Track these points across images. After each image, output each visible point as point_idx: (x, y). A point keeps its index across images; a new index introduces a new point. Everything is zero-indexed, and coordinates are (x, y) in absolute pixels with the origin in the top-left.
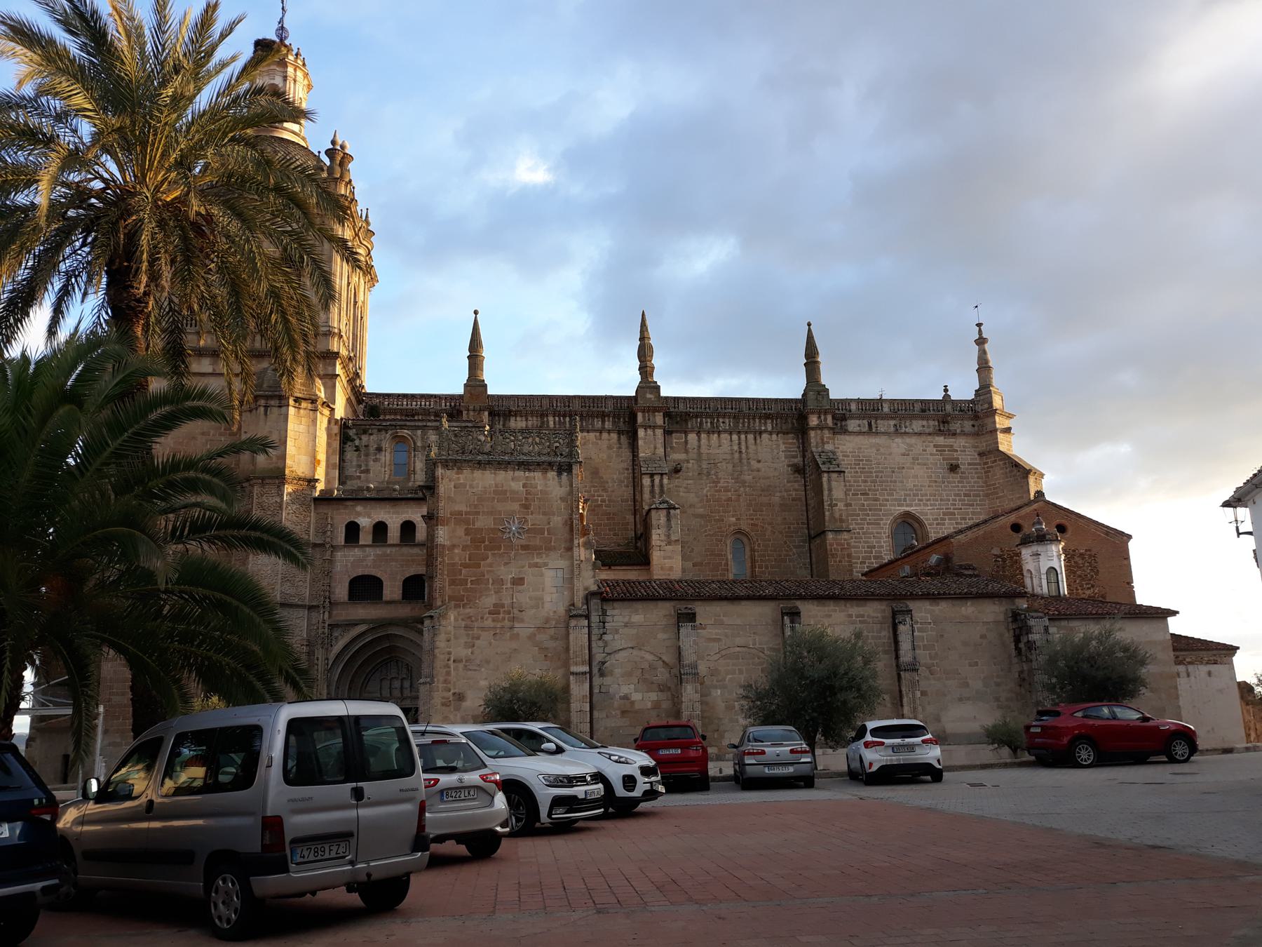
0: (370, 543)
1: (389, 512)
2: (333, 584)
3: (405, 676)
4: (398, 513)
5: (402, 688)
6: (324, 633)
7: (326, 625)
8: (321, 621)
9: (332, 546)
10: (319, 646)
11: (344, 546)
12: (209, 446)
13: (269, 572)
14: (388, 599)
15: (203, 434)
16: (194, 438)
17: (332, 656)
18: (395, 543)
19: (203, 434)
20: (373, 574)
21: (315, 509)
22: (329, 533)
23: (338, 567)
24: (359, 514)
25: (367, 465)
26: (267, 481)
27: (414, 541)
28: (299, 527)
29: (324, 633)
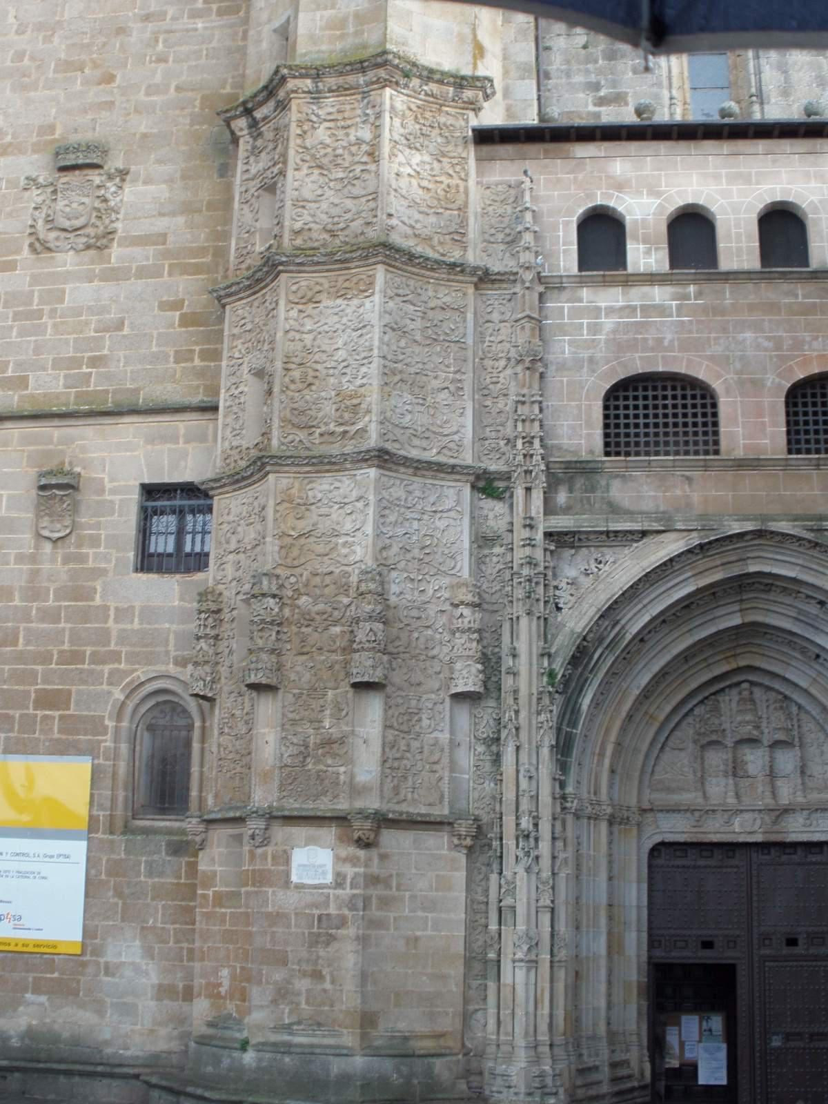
0: (665, 267)
1: (717, 177)
2: (550, 403)
3: (780, 736)
4: (747, 179)
5: (772, 775)
6: (531, 562)
7: (539, 536)
8: (518, 521)
9: (540, 279)
10: (518, 609)
11: (581, 282)
12: (160, 46)
13: (341, 354)
14: (740, 453)
15: (147, 18)
16: (121, 31)
17: (563, 644)
18: (746, 266)
19: (147, 18)
20: (681, 369)
21: (480, 173)
22: (528, 238)
23: (562, 349)
24: (620, 186)
25: (614, 84)
26: (332, 81)
27: (804, 261)
28: (433, 219)
29: (531, 562)
